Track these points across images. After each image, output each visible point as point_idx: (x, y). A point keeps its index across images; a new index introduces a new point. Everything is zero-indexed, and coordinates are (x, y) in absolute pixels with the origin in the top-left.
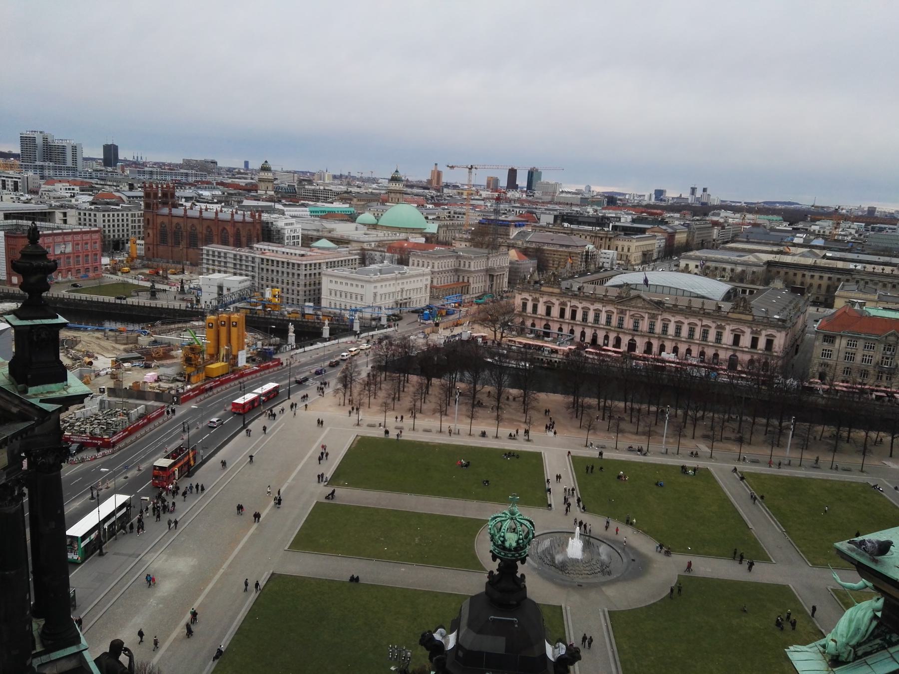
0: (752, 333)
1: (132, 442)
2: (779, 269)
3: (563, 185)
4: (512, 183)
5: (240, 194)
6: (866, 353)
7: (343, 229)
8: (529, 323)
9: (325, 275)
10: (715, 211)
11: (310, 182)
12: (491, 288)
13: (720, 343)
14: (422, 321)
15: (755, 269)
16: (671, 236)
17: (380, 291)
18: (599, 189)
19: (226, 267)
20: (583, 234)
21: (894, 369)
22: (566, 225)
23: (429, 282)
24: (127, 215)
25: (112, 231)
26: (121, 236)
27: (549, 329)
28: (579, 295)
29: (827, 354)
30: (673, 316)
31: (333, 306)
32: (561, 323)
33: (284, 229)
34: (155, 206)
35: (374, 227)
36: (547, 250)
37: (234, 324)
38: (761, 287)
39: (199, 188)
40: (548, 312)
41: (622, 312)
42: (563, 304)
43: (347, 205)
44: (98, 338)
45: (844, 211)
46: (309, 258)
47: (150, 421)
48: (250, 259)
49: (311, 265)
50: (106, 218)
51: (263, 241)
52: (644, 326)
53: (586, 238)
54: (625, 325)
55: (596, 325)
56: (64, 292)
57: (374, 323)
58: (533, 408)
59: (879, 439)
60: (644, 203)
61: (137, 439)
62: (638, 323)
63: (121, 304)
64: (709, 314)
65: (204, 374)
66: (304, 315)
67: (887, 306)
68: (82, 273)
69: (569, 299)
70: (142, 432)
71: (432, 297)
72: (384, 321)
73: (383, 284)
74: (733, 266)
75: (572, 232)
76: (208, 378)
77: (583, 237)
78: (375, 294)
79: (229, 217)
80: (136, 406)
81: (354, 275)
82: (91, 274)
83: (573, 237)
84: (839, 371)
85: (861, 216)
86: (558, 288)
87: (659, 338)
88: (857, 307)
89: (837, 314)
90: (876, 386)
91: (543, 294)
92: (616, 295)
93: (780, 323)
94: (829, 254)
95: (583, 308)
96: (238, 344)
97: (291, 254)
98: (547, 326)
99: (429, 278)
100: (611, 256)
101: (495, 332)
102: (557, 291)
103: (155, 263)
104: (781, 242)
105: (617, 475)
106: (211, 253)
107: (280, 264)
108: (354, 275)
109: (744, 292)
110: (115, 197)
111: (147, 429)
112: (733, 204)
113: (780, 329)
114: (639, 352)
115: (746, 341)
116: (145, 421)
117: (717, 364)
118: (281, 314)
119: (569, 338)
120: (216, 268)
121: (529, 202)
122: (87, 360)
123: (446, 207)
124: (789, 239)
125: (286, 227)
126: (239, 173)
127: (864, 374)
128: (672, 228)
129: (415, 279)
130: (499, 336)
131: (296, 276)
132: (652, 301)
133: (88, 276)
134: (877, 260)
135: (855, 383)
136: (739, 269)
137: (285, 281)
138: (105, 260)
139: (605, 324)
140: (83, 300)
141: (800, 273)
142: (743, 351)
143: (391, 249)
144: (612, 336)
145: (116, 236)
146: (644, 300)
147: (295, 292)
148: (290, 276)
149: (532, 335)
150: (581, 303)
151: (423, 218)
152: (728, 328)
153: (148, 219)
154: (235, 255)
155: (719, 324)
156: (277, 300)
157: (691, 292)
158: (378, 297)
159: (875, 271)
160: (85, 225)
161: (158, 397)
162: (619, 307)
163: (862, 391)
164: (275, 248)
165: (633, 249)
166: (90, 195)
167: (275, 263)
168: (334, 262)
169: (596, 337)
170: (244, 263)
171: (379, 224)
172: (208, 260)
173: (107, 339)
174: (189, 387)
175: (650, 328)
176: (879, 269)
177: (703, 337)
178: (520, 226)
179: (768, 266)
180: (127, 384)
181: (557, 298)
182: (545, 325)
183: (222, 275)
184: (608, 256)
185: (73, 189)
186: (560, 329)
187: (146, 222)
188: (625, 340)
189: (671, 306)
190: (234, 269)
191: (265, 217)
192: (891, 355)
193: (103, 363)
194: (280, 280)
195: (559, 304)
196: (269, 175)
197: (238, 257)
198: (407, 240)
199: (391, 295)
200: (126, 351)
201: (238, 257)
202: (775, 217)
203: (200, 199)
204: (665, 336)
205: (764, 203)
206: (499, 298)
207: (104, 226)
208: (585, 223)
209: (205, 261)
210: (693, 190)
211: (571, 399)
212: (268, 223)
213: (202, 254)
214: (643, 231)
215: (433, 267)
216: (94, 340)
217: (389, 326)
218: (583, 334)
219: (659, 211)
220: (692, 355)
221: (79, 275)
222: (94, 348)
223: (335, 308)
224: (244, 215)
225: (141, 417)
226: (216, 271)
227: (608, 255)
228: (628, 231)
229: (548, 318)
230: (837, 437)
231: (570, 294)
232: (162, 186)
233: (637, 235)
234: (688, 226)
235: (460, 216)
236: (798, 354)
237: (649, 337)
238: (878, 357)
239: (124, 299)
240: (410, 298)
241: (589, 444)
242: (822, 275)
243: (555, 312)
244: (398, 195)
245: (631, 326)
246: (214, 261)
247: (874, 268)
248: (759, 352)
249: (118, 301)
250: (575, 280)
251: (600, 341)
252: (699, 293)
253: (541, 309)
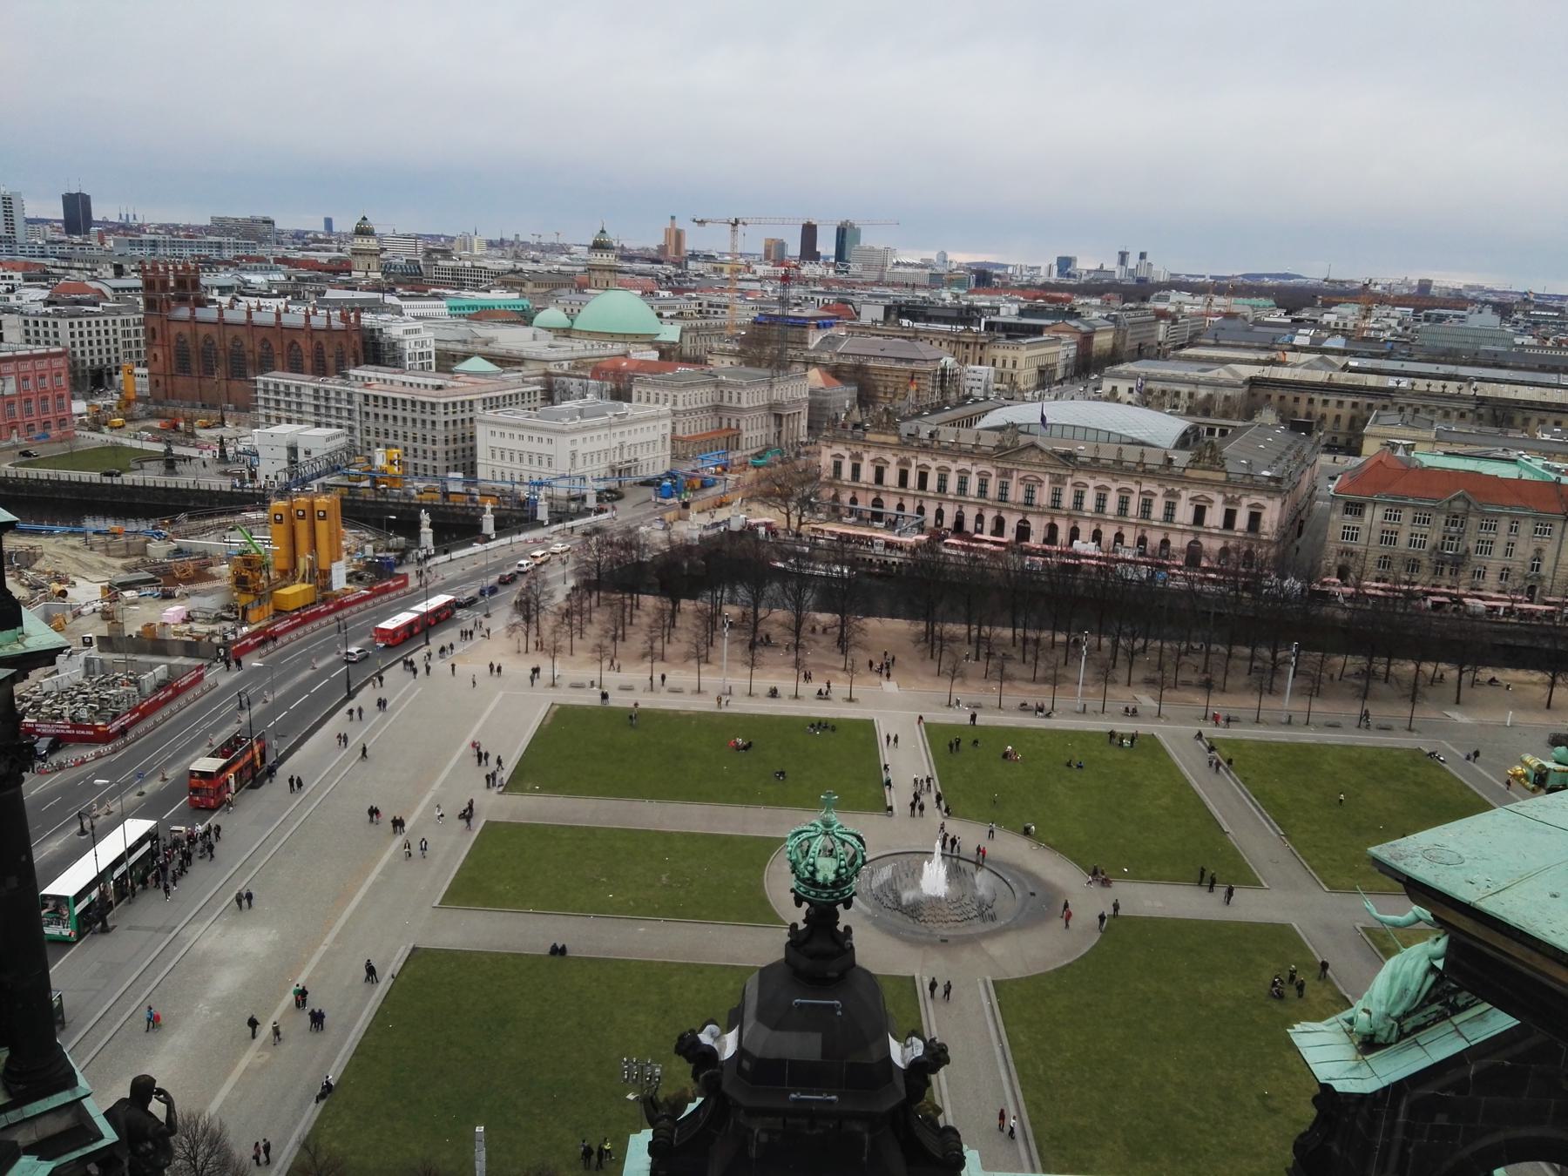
0: (1226, 501)
1: (148, 731)
2: (1270, 392)
3: (899, 252)
4: (809, 251)
5: (319, 279)
6: (1416, 530)
7: (510, 338)
8: (846, 498)
9: (481, 421)
10: (1161, 293)
11: (446, 254)
12: (779, 438)
13: (1171, 522)
14: (659, 500)
15: (1229, 392)
16: (1087, 338)
17: (582, 448)
18: (961, 257)
19: (301, 412)
21: (1463, 556)
22: (905, 322)
23: (668, 430)
24: (114, 322)
25: (87, 353)
26: (105, 362)
27: (882, 507)
28: (931, 446)
29: (1350, 534)
30: (1091, 478)
31: (498, 478)
32: (902, 496)
33: (403, 340)
34: (165, 304)
35: (566, 333)
36: (875, 368)
37: (321, 514)
38: (1240, 424)
39: (244, 269)
40: (879, 479)
41: (1006, 473)
42: (904, 462)
43: (516, 295)
44: (74, 548)
45: (1378, 288)
46: (451, 392)
47: (178, 692)
48: (344, 396)
49: (454, 404)
50: (76, 330)
51: (366, 363)
52: (1043, 496)
54: (1011, 497)
55: (962, 498)
56: (6, 466)
57: (573, 505)
58: (858, 644)
59: (1438, 675)
60: (1040, 281)
61: (156, 725)
63: (112, 485)
64: (1152, 472)
65: (271, 605)
66: (446, 495)
67: (1450, 449)
68: (38, 432)
70: (166, 712)
71: (675, 457)
72: (591, 502)
73: (588, 435)
74: (1192, 388)
75: (916, 335)
76: (279, 613)
77: (936, 343)
78: (574, 454)
79: (301, 322)
80: (152, 667)
81: (534, 422)
82: (54, 432)
83: (918, 344)
84: (1371, 564)
85: (1408, 296)
87: (1069, 516)
88: (1400, 453)
89: (1367, 467)
90: (1433, 586)
91: (869, 445)
92: (995, 444)
93: (1272, 484)
94: (1354, 363)
95: (938, 469)
96: (330, 549)
97: (419, 385)
98: (877, 502)
99: (668, 422)
100: (984, 377)
101: (788, 515)
102: (893, 439)
103: (170, 409)
104: (1271, 344)
105: (1002, 752)
106: (271, 387)
107: (399, 405)
108: (534, 422)
109: (1211, 432)
110: (89, 290)
111: (174, 706)
112: (1191, 280)
113: (1271, 495)
114: (1035, 541)
115: (1215, 517)
116: (170, 692)
117: (1166, 558)
118: (405, 494)
119: (916, 522)
120: (283, 414)
121: (841, 282)
122: (57, 587)
123: (694, 295)
124: (1286, 339)
125: (407, 337)
126: (316, 240)
127: (1413, 565)
128: (1087, 323)
129: (644, 425)
130: (794, 521)
131: (429, 426)
133: (48, 436)
134: (1434, 371)
135: (1397, 582)
136: (1202, 393)
137: (410, 435)
138: (79, 406)
140: (42, 481)
141: (1304, 398)
142: (1210, 535)
143: (597, 372)
144: (989, 516)
145: (97, 362)
146: (1042, 451)
147: (429, 454)
148: (419, 425)
149: (853, 519)
150: (935, 460)
152: (1185, 495)
153: (153, 329)
154: (316, 391)
155: (1170, 488)
156: (396, 469)
157: (1121, 435)
158: (579, 459)
159: (1431, 389)
160: (38, 342)
161: (191, 649)
162: (1000, 465)
163: (1410, 595)
164: (387, 376)
165: (1021, 364)
166: (43, 287)
167: (390, 403)
168: (497, 398)
169: (963, 517)
170: (333, 403)
171: (575, 327)
172: (267, 400)
173: (91, 549)
174: (245, 629)
175: (1054, 501)
176: (1437, 386)
177: (1144, 511)
178: (825, 326)
179: (1250, 387)
180: (133, 628)
182: (874, 500)
183: (294, 427)
184: (979, 376)
185: (11, 278)
186: (901, 507)
187: (150, 334)
188: (1012, 522)
189: (1088, 460)
190: (316, 415)
191: (367, 319)
192: (1458, 532)
193: (87, 592)
194: (400, 433)
195: (898, 463)
196: (371, 244)
197: (322, 394)
198: (626, 355)
199: (602, 455)
200: (126, 568)
201: (322, 394)
202: (1262, 301)
203: (245, 290)
204: (1079, 513)
205: (1243, 276)
206: (792, 455)
207: (73, 344)
208: (938, 319)
209: (261, 403)
210: (1123, 257)
211: (922, 626)
212: (373, 330)
213: (256, 391)
214: (1038, 331)
215: (675, 403)
216: (67, 552)
217: (600, 511)
218: (940, 514)
219: (1064, 295)
220: (1126, 544)
221: (33, 435)
222: (67, 566)
223: (503, 481)
224: (329, 317)
225: (162, 686)
226: (283, 421)
227: (978, 375)
228: (1013, 332)
229: (878, 487)
230: (1368, 674)
231: (915, 444)
232: (175, 268)
233: (1028, 337)
234: (1115, 320)
235: (719, 310)
236: (1303, 537)
237: (1053, 516)
238: (1435, 537)
239: (118, 475)
240: (636, 460)
241: (953, 701)
242: (1342, 399)
243: (891, 477)
244: (607, 274)
245: (1021, 498)
246: (278, 402)
247: (1429, 386)
248: (1238, 534)
249: (107, 480)
251: (969, 525)
252: (1134, 436)
253: (867, 473)
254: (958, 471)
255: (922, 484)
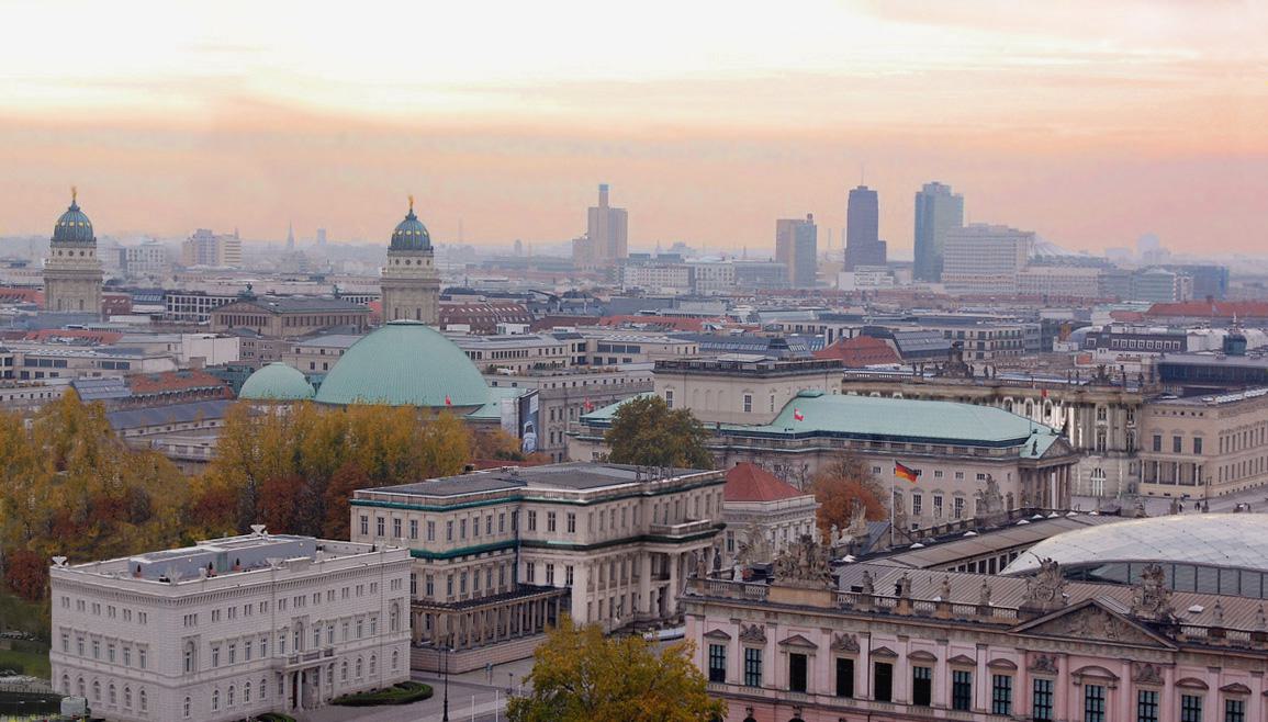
20: (1016, 399)
23: (405, 593)
30: (1212, 669)
41: (1043, 664)
42: (845, 645)
53: (1029, 412)
62: (1100, 699)
69: (863, 627)
86: (823, 590)
91: (774, 611)
92: (1019, 603)
95: (911, 657)
102: (821, 600)
123: (571, 330)
132: (1136, 620)
139: (989, 708)
146: (1110, 616)
151: (472, 370)
162: (1031, 646)
171: (319, 398)
181: (822, 624)
189: (1204, 633)
195: (833, 647)
215: (431, 537)
229: (797, 697)
231: (865, 608)
243: (821, 674)
244: (419, 296)
250: (900, 557)
254: (950, 661)
255: (883, 688)
